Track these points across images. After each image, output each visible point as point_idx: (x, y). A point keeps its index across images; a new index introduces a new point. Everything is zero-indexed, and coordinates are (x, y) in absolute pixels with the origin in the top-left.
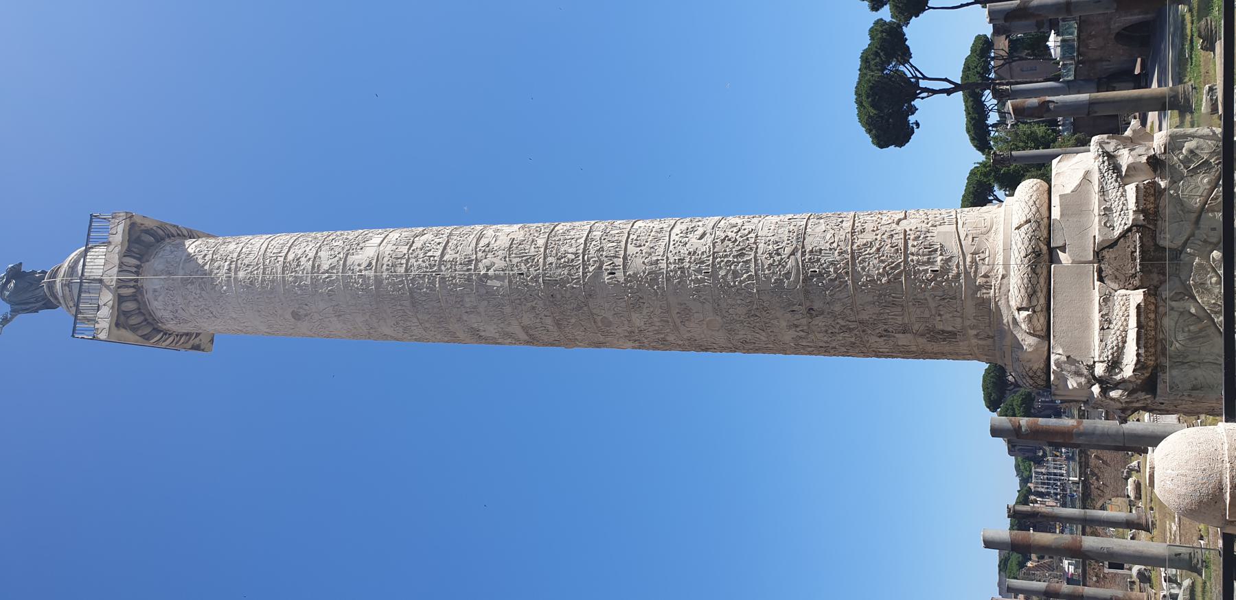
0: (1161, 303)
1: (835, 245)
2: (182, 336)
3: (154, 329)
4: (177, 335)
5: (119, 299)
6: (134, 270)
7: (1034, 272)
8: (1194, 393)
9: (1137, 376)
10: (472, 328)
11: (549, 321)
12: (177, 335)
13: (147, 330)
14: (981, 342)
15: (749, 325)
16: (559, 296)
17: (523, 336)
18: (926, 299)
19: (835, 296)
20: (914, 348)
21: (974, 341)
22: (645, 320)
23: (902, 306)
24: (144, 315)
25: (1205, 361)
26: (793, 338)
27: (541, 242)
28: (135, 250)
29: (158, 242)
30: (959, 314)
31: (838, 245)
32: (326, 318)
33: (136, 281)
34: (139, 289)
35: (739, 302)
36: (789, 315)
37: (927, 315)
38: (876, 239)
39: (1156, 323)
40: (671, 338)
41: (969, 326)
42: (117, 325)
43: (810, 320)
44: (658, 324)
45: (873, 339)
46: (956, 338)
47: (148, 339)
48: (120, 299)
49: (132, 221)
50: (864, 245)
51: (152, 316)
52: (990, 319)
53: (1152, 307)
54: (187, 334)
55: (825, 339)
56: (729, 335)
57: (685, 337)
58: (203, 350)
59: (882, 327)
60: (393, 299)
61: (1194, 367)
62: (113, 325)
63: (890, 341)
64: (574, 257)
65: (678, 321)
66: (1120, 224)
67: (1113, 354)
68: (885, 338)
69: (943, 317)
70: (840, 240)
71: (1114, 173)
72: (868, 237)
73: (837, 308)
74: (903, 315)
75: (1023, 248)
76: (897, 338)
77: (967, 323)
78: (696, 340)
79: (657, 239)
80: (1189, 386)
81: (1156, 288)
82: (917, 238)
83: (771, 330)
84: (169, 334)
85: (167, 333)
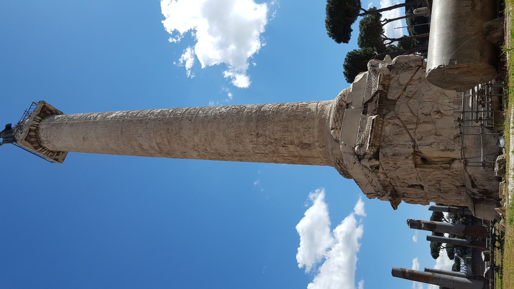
0: (385, 121)
1: (271, 109)
2: (50, 152)
3: (40, 145)
4: (48, 151)
5: (29, 130)
6: (38, 121)
7: (338, 112)
8: (393, 157)
9: (370, 149)
10: (140, 144)
11: (165, 140)
12: (48, 151)
13: (36, 145)
14: (321, 150)
15: (235, 141)
16: (170, 129)
17: (157, 148)
18: (300, 129)
19: (267, 128)
20: (296, 154)
21: (318, 149)
23: (291, 132)
24: (37, 138)
25: (400, 143)
26: (252, 148)
27: (171, 111)
28: (42, 115)
29: (52, 114)
30: (312, 135)
31: (273, 109)
32: (93, 139)
33: (38, 125)
34: (38, 128)
35: (232, 130)
36: (250, 136)
37: (299, 136)
38: (287, 107)
39: (382, 129)
40: (208, 149)
41: (316, 141)
42: (26, 139)
43: (257, 139)
44: (204, 141)
45: (281, 148)
46: (311, 147)
47: (36, 149)
48: (30, 130)
49: (45, 105)
50: (282, 109)
51: (39, 139)
52: (323, 137)
53: (381, 122)
54: (52, 152)
55: (263, 148)
57: (213, 148)
58: (59, 162)
59: (283, 142)
60: (115, 131)
61: (395, 147)
62: (24, 139)
63: (287, 149)
64: (179, 114)
65: (210, 139)
66: (373, 91)
67: (362, 141)
68: (285, 148)
69: (306, 136)
70: (274, 108)
71: (374, 72)
72: (284, 107)
73: (267, 133)
74: (291, 136)
75: (336, 104)
76: (289, 147)
77: (315, 139)
78: (217, 150)
79: (210, 109)
80: (391, 154)
81: (385, 115)
82: (301, 107)
83: (243, 144)
84: (45, 149)
85: (44, 148)
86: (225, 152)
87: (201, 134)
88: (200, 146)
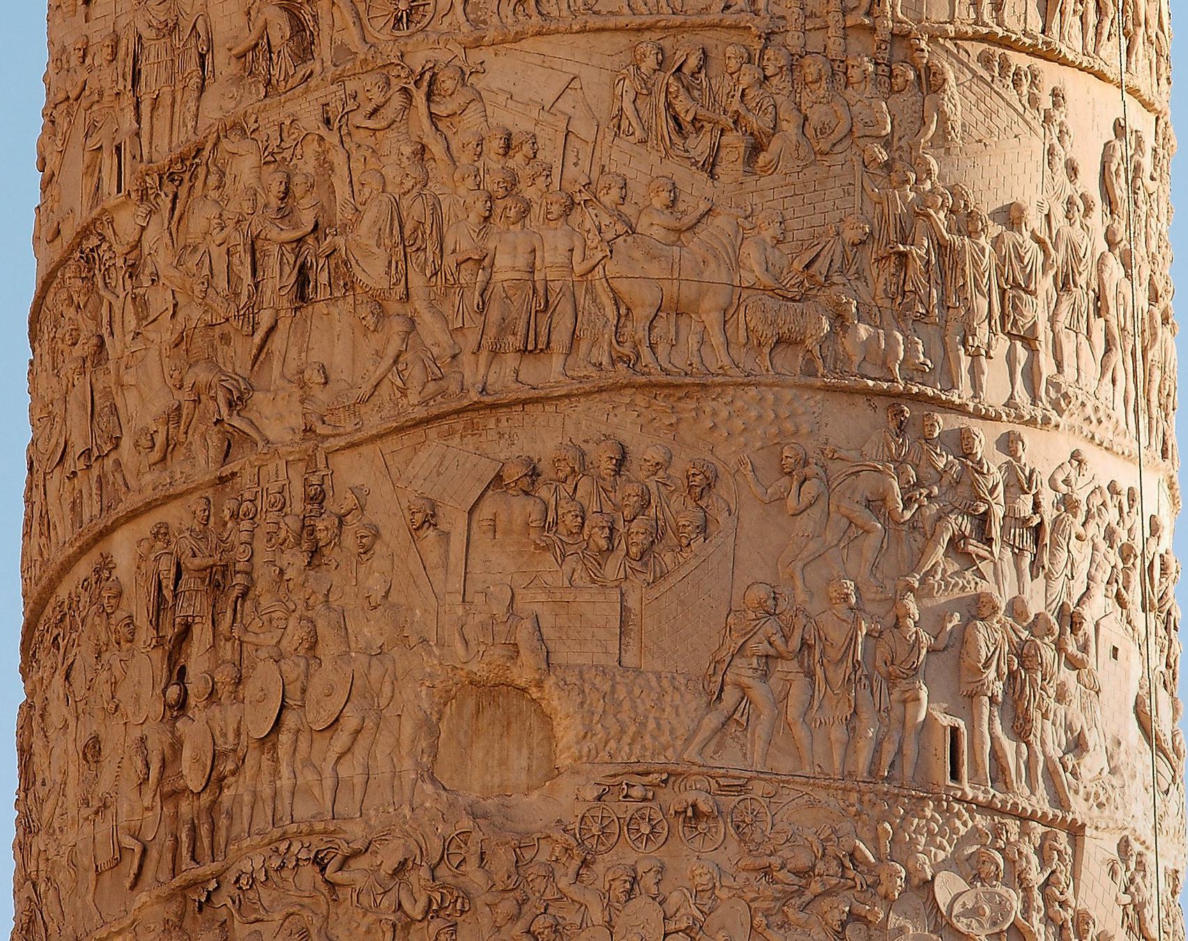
22: (549, 154)
44: (507, 265)
56: (389, 858)
86: (268, 742)
87: (654, 225)
88: (398, 147)
